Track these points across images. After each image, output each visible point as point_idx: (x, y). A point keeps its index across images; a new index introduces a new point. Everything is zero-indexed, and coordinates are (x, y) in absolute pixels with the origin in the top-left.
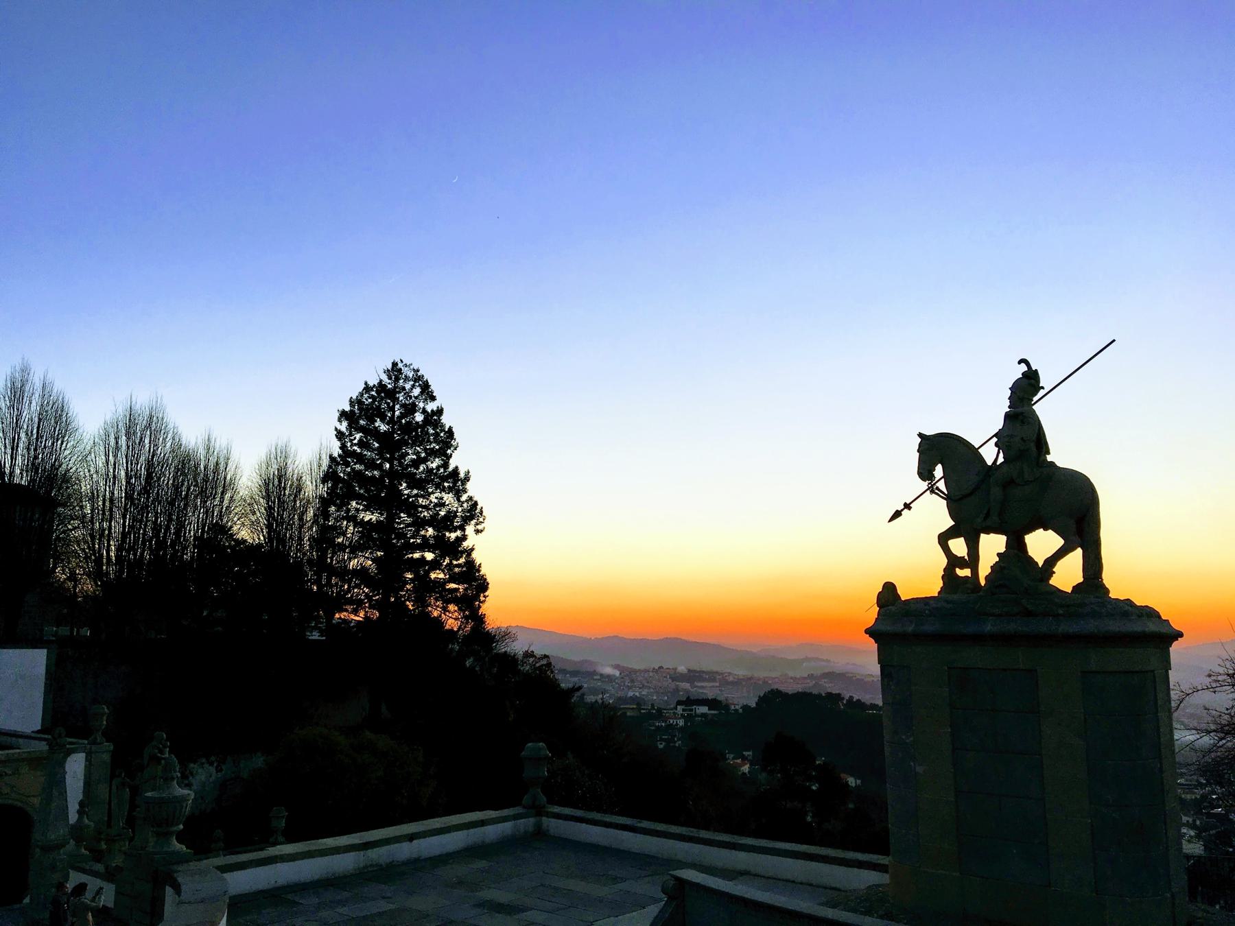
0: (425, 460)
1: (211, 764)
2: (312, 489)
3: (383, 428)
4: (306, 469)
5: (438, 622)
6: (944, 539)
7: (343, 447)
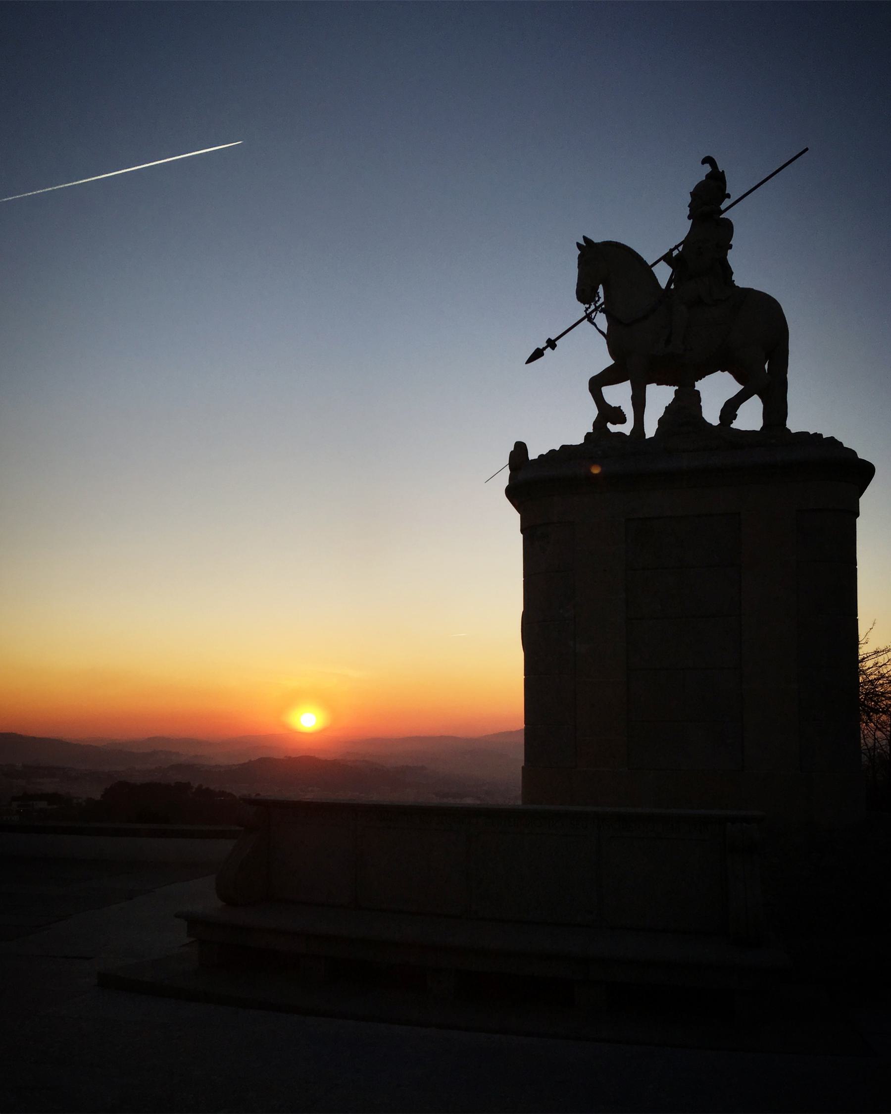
6: (596, 385)
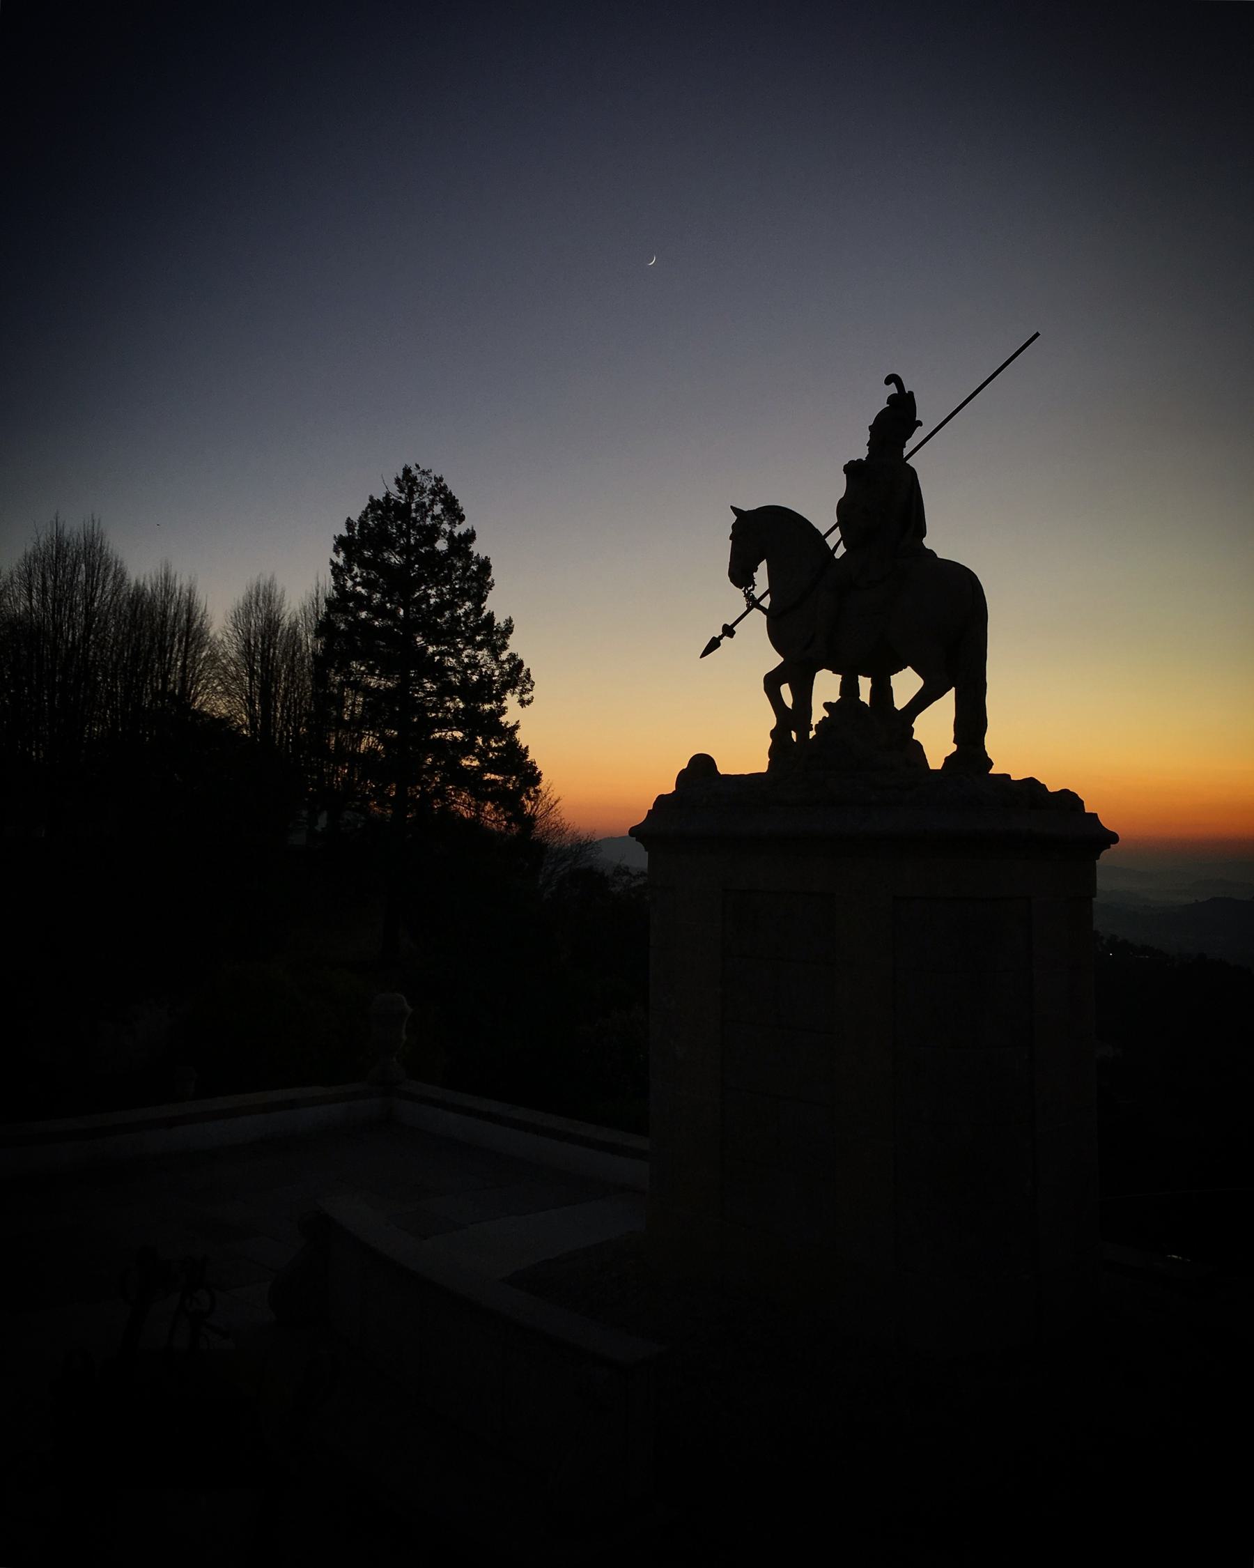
0: (452, 606)
2: (310, 642)
3: (395, 559)
5: (475, 825)
6: (772, 683)
7: (340, 587)
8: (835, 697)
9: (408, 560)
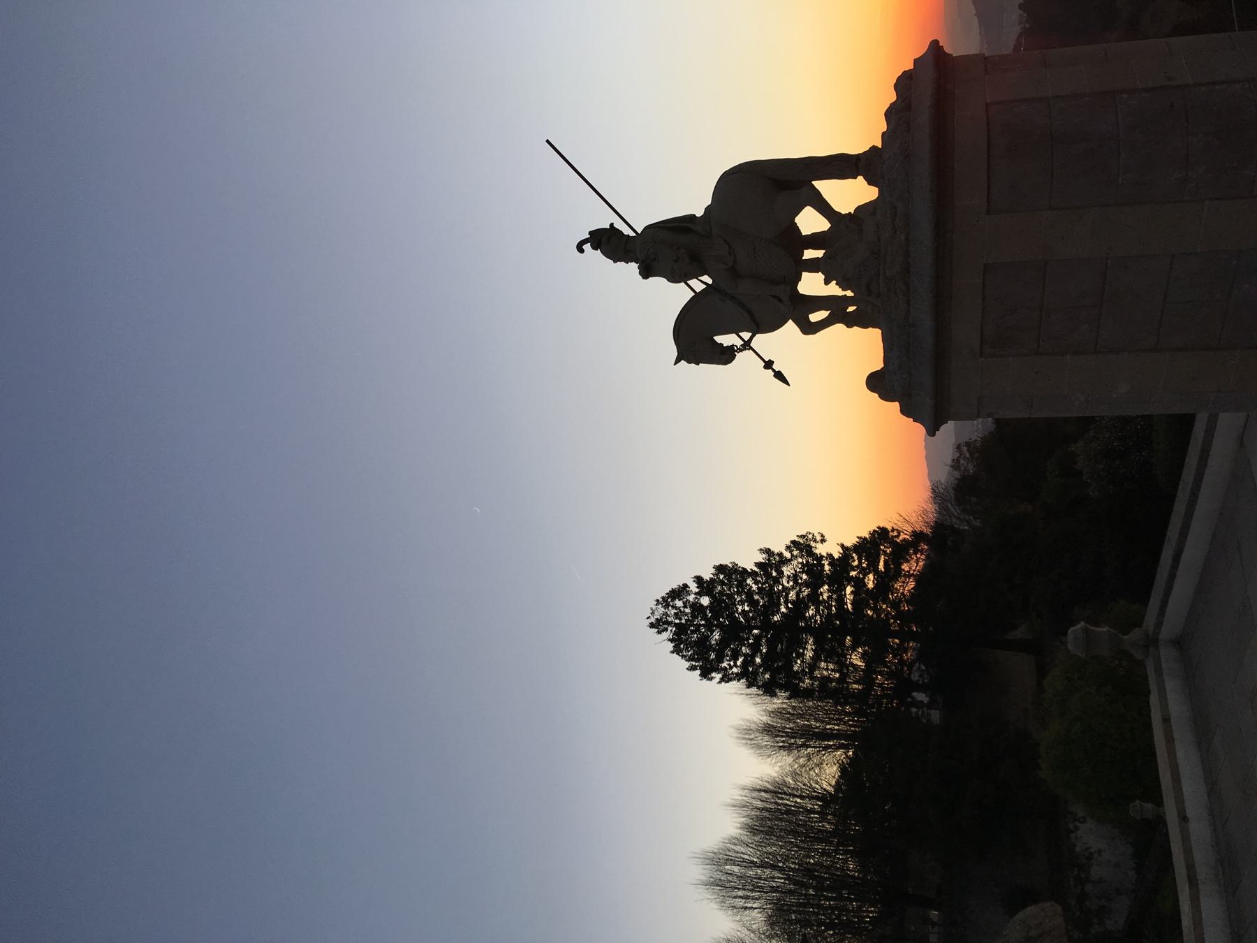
0: (750, 594)
1: (1077, 828)
2: (780, 701)
3: (716, 635)
4: (759, 708)
5: (920, 579)
6: (809, 329)
7: (738, 677)
8: (820, 277)
9: (717, 626)
